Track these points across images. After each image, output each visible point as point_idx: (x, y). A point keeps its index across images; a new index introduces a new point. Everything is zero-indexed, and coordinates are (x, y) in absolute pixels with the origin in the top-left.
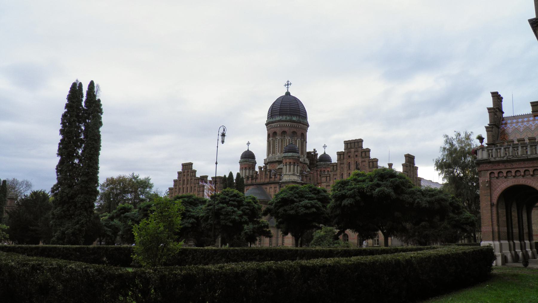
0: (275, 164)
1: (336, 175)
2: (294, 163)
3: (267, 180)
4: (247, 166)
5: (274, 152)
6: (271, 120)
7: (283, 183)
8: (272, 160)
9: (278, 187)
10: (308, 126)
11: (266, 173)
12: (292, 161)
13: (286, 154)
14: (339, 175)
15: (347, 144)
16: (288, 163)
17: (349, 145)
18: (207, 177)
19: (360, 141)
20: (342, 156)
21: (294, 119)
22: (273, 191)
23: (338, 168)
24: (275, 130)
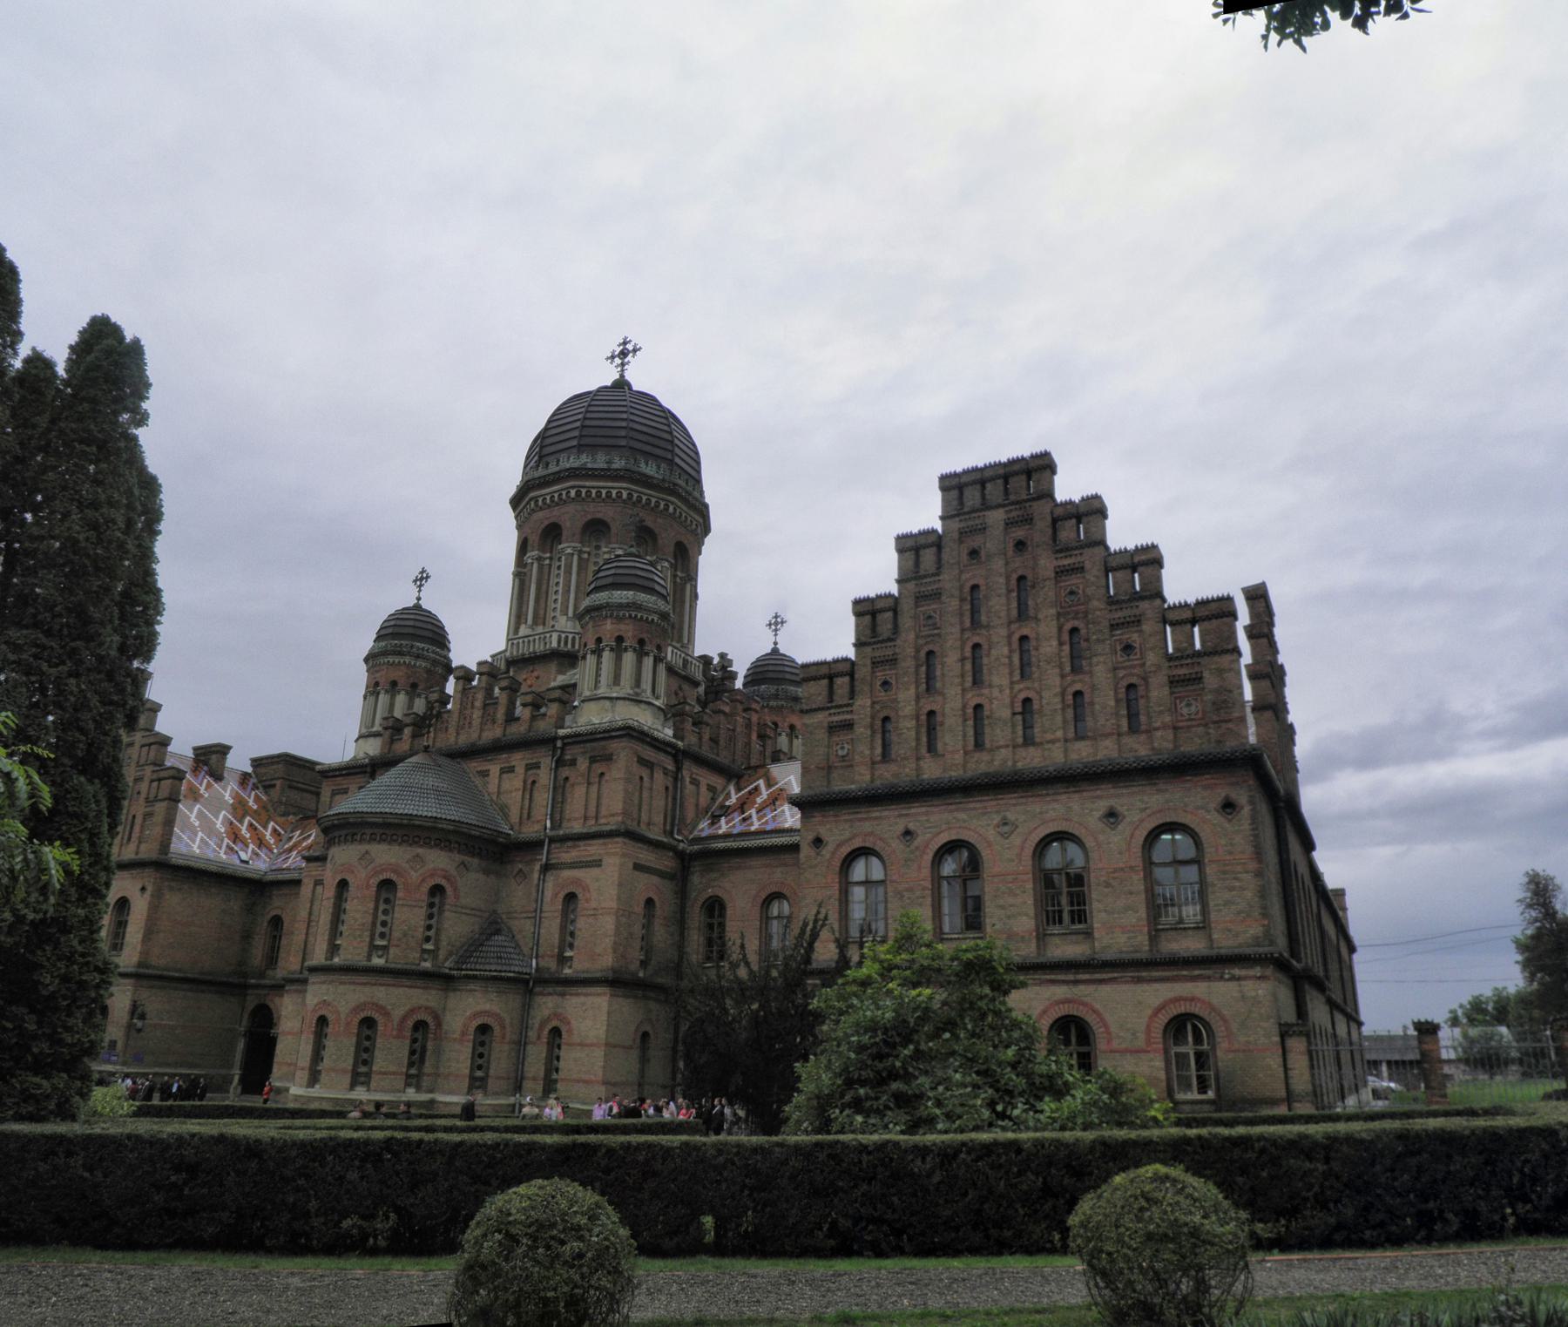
0: (539, 670)
1: (892, 661)
2: (641, 642)
3: (493, 733)
4: (398, 674)
5: (540, 619)
6: (541, 472)
7: (578, 739)
8: (526, 650)
9: (547, 762)
10: (707, 529)
11: (489, 691)
12: (629, 631)
13: (602, 597)
14: (908, 664)
15: (961, 488)
16: (608, 641)
18: (223, 750)
19: (1040, 467)
20: (928, 557)
21: (649, 469)
22: (514, 783)
23: (906, 621)
24: (554, 515)
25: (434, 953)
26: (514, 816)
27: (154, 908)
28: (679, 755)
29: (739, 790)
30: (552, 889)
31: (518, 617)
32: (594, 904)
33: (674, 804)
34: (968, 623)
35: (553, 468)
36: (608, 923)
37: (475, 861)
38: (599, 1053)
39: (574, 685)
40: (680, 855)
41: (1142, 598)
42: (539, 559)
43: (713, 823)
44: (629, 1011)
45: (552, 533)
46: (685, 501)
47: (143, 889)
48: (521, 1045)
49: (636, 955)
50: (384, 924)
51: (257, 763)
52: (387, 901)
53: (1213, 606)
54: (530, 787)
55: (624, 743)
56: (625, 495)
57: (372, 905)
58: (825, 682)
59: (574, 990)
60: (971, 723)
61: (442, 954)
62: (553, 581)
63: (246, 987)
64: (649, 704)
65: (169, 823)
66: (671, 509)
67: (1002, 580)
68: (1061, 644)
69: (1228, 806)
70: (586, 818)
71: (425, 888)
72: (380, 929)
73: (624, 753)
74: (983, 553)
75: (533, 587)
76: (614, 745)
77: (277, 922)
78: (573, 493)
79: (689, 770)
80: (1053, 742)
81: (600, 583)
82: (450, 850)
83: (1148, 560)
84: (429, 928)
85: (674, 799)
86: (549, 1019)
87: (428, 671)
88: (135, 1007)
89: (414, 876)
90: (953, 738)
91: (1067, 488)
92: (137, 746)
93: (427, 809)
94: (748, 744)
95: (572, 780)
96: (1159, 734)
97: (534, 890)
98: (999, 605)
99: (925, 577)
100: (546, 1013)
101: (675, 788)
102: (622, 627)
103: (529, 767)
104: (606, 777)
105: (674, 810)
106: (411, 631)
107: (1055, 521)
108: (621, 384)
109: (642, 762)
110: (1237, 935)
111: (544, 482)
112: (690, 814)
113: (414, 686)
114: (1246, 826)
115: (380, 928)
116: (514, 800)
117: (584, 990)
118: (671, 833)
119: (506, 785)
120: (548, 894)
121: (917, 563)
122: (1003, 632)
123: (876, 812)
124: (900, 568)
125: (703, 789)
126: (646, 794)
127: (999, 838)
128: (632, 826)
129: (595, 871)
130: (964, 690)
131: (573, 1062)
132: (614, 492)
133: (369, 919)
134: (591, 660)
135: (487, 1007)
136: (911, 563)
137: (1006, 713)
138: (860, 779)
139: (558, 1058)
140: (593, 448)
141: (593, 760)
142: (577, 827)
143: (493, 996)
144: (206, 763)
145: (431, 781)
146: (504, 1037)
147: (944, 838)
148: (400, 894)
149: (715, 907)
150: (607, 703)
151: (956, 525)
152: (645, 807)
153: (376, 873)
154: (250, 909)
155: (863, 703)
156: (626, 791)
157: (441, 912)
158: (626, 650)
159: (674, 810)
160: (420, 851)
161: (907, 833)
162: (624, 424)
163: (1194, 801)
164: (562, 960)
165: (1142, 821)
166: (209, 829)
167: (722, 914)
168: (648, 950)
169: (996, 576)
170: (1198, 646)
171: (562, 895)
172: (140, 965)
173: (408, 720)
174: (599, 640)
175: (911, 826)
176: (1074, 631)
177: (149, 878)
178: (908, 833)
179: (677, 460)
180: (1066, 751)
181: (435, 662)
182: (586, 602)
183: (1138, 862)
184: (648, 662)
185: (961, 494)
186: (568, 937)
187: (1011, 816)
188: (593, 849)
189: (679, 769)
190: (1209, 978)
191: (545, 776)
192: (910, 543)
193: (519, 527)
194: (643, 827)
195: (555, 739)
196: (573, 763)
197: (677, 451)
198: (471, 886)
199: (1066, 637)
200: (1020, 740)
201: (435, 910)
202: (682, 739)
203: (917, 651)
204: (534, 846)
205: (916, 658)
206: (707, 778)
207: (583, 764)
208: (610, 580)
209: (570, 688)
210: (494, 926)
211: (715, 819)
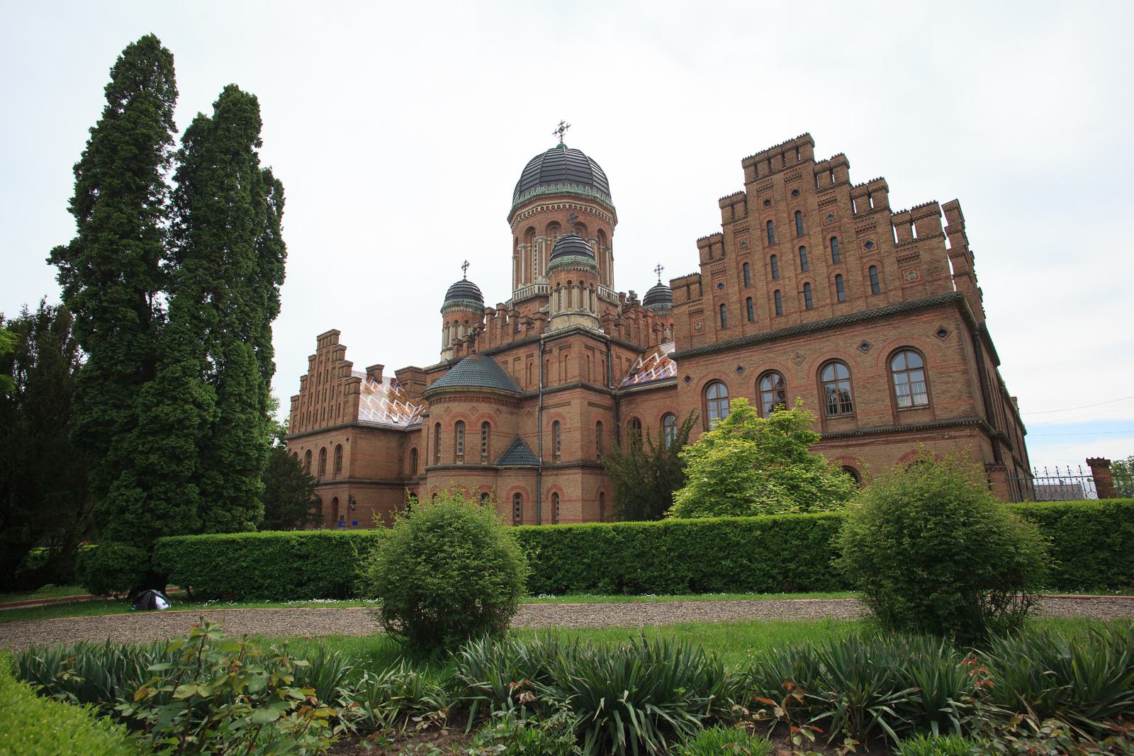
2: (581, 283)
3: (508, 340)
4: (457, 317)
6: (522, 199)
7: (552, 338)
8: (521, 297)
9: (537, 353)
10: (615, 222)
12: (574, 277)
13: (558, 260)
15: (755, 165)
16: (564, 283)
17: (763, 168)
19: (805, 142)
20: (739, 208)
22: (521, 365)
23: (729, 248)
25: (488, 457)
26: (523, 383)
27: (354, 448)
28: (608, 343)
29: (644, 360)
30: (547, 419)
31: (517, 280)
32: (568, 426)
33: (608, 369)
34: (767, 243)
35: (527, 197)
36: (577, 435)
37: (504, 409)
38: (579, 505)
39: (548, 312)
40: (614, 397)
41: (876, 212)
42: (525, 247)
43: (631, 378)
44: (594, 481)
45: (531, 231)
46: (601, 205)
47: (348, 439)
48: (538, 502)
49: (594, 452)
50: (461, 444)
51: (398, 373)
52: (461, 432)
53: (924, 209)
54: (529, 367)
55: (577, 337)
56: (567, 207)
57: (453, 434)
58: (685, 288)
59: (562, 472)
60: (773, 301)
61: (492, 458)
62: (533, 258)
63: (403, 485)
64: (589, 316)
65: (356, 405)
66: (594, 211)
67: (785, 215)
68: (825, 248)
69: (942, 332)
70: (560, 381)
71: (480, 424)
72: (459, 447)
73: (577, 343)
74: (772, 201)
75: (523, 263)
76: (571, 339)
77: (414, 451)
78: (539, 209)
79: (615, 350)
80: (824, 306)
81: (557, 253)
82: (491, 403)
83: (878, 188)
84: (484, 444)
85: (608, 367)
86: (551, 488)
87: (473, 314)
88: (350, 497)
89: (473, 418)
90: (763, 311)
91: (822, 153)
92: (337, 369)
93: (475, 382)
94: (647, 335)
95: (551, 361)
96: (892, 293)
97: (537, 420)
98: (785, 230)
99: (739, 220)
100: (550, 485)
101: (608, 361)
102: (570, 275)
103: (528, 357)
104: (569, 357)
105: (608, 373)
106: (462, 293)
107: (815, 175)
108: (561, 146)
109: (587, 347)
110: (952, 411)
111: (524, 205)
112: (618, 374)
113: (467, 322)
114: (954, 343)
115: (458, 446)
116: (522, 375)
117: (568, 471)
118: (608, 385)
119: (517, 367)
120: (544, 422)
121: (733, 213)
122: (789, 245)
123: (720, 358)
124: (723, 218)
125: (624, 360)
126: (591, 365)
127: (795, 366)
128: (586, 382)
129: (567, 408)
130: (767, 283)
131: (564, 509)
132: (561, 205)
133: (453, 441)
134: (555, 295)
135: (518, 484)
136: (730, 214)
137: (795, 293)
138: (710, 340)
139: (558, 509)
140: (548, 182)
141: (561, 349)
142: (556, 385)
143: (521, 478)
144: (372, 375)
145: (477, 368)
146: (528, 499)
147: (762, 369)
148: (467, 428)
149: (637, 423)
150: (566, 317)
151: (755, 186)
152: (592, 372)
153: (454, 418)
154: (401, 445)
155: (708, 298)
156: (580, 363)
157: (489, 435)
158: (573, 288)
159: (608, 373)
160: (475, 404)
161: (740, 368)
162: (564, 167)
163: (920, 331)
164: (555, 457)
165: (884, 347)
166: (378, 408)
167: (640, 427)
168: (600, 449)
169: (782, 214)
170: (915, 236)
171: (551, 423)
172: (351, 477)
173: (464, 339)
174: (558, 284)
175: (741, 365)
176: (833, 239)
177: (349, 433)
178: (740, 368)
179: (595, 183)
180: (833, 311)
181: (476, 308)
182: (550, 264)
183: (883, 372)
184: (586, 293)
185: (756, 168)
186: (557, 443)
187: (801, 352)
188: (566, 396)
189: (609, 350)
190: (934, 439)
191: (536, 361)
192: (728, 202)
193: (513, 232)
194: (592, 382)
195: (539, 340)
196: (551, 351)
197: (594, 178)
198: (503, 420)
199: (828, 243)
200: (804, 308)
201: (486, 435)
202: (609, 334)
203: (738, 264)
204: (534, 397)
205: (737, 268)
206: (626, 354)
207: (556, 351)
208: (561, 251)
209: (546, 313)
210: (518, 442)
211: (632, 376)
